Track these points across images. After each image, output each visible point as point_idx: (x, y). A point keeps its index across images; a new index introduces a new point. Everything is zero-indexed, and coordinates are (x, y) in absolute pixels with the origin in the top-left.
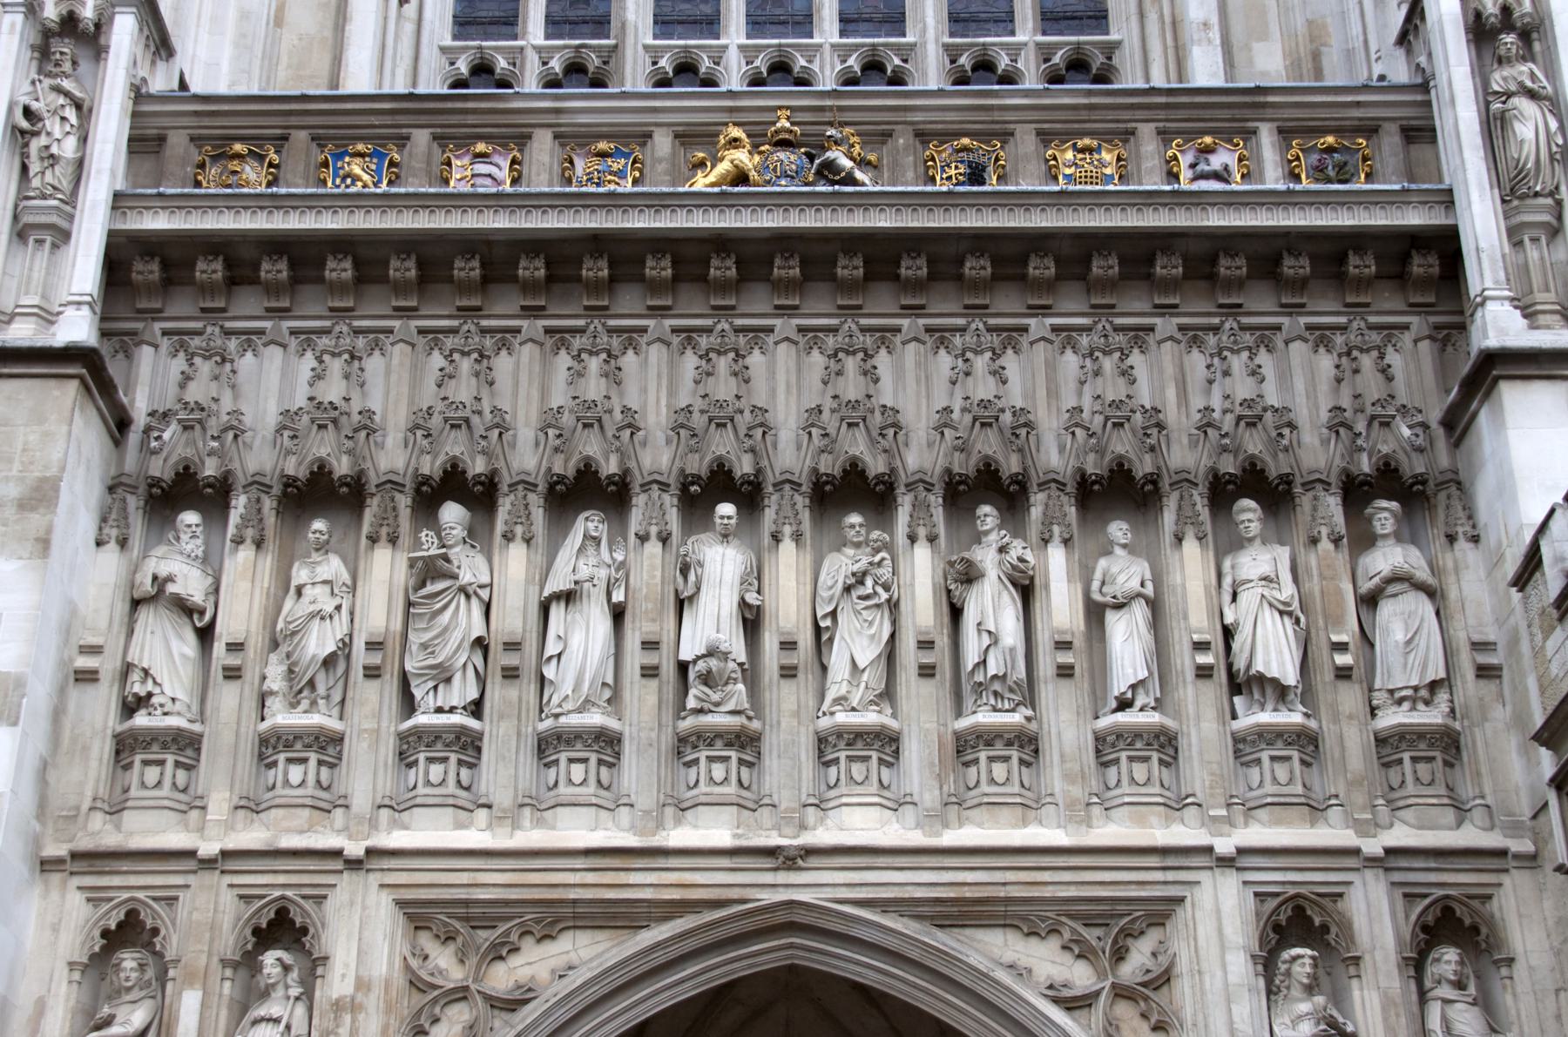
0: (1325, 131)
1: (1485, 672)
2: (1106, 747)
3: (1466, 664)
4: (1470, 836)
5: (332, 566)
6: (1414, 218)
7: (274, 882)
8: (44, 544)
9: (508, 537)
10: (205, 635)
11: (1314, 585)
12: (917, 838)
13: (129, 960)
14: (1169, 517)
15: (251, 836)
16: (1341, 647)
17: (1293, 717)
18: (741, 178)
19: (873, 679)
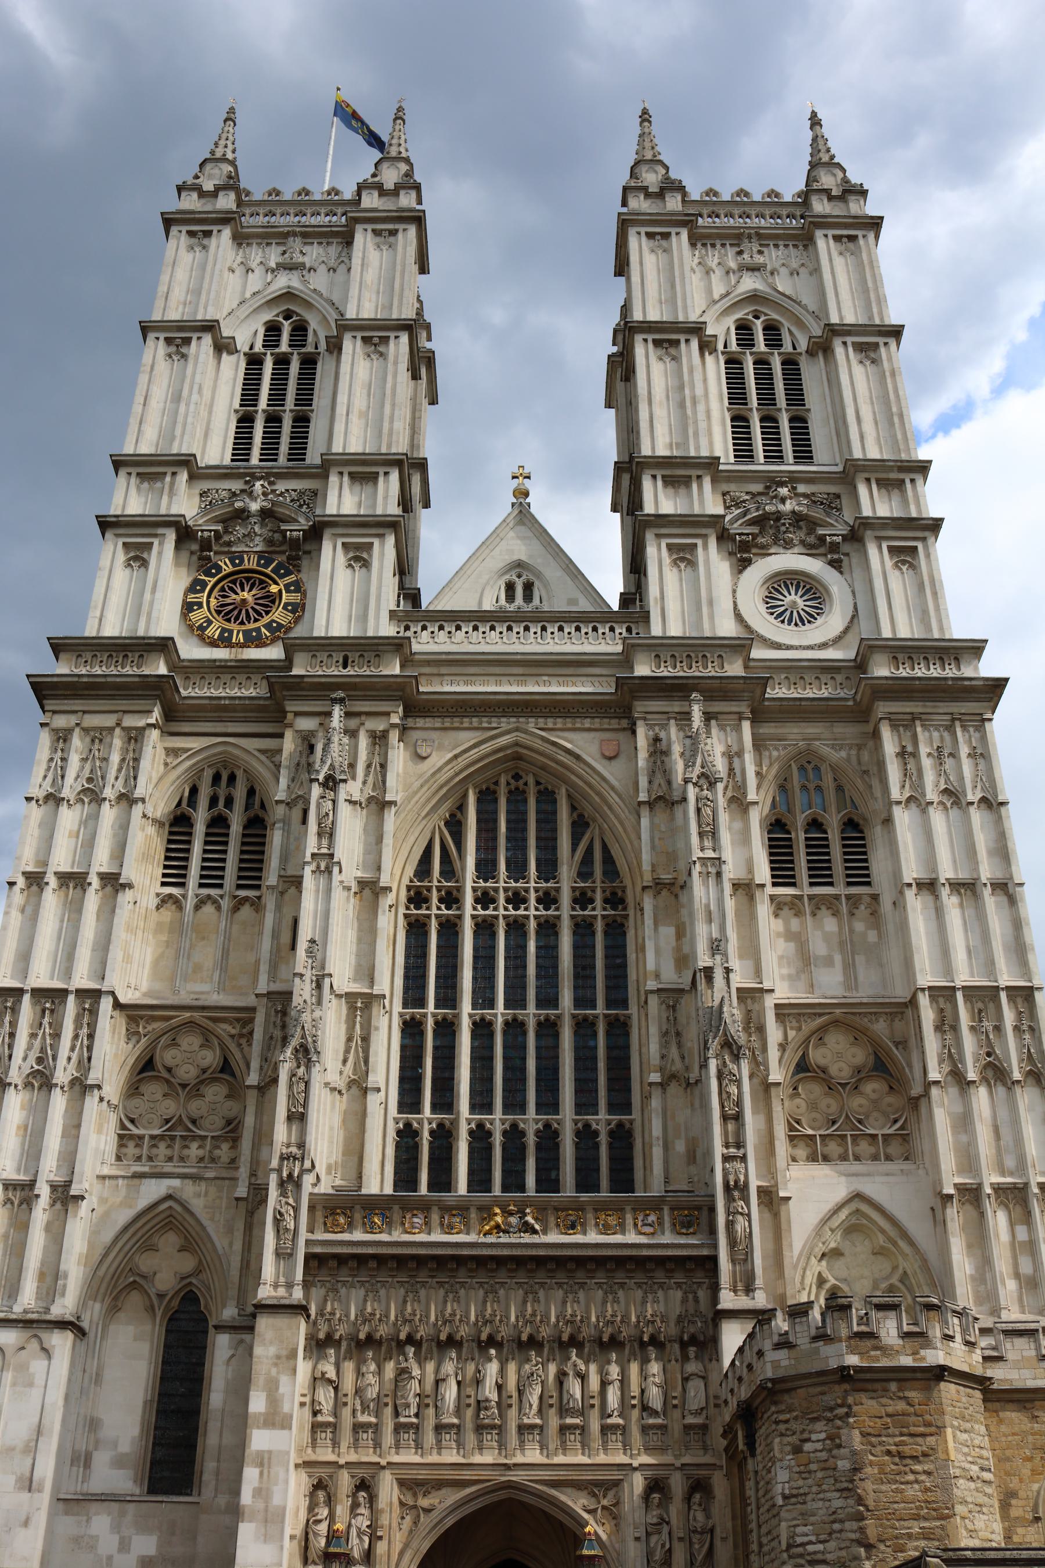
0: (684, 1209)
1: (716, 1406)
2: (605, 1429)
3: (712, 1401)
4: (707, 1459)
5: (373, 1367)
6: (705, 1252)
7: (361, 1473)
8: (294, 1371)
9: (426, 1359)
10: (336, 1389)
11: (668, 1376)
12: (545, 1461)
13: (321, 1495)
14: (627, 1351)
15: (353, 1457)
16: (675, 1398)
17: (659, 1421)
18: (497, 1226)
19: (535, 1407)
